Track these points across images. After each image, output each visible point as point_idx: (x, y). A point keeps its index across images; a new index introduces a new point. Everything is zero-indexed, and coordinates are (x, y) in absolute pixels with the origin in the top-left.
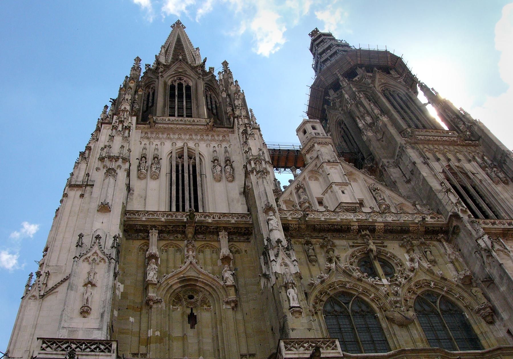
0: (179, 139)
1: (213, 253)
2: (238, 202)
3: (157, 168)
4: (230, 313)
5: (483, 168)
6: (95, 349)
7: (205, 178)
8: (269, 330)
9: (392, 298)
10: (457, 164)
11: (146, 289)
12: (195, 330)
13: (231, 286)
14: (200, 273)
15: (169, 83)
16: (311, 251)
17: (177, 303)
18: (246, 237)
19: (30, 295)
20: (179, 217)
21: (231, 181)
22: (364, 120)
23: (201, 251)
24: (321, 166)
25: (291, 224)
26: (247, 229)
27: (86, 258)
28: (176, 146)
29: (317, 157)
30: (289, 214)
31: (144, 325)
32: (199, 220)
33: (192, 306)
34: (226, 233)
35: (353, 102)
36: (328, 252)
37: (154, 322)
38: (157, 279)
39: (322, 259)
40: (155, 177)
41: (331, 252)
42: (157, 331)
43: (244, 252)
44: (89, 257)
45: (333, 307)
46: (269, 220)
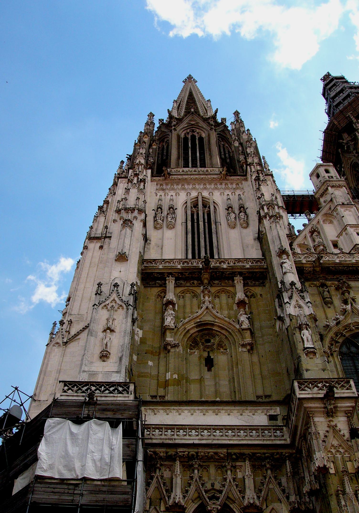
0: (194, 188)
1: (229, 297)
2: (252, 247)
3: (172, 217)
4: (246, 356)
6: (114, 390)
7: (219, 225)
8: (285, 371)
12: (212, 372)
15: (182, 136)
16: (326, 293)
17: (194, 347)
19: (54, 342)
20: (195, 264)
21: (246, 228)
23: (217, 296)
24: (335, 209)
25: (306, 267)
27: (105, 306)
28: (191, 196)
30: (303, 257)
32: (214, 266)
33: (209, 350)
34: (241, 278)
36: (343, 294)
37: (171, 366)
38: (174, 324)
39: (337, 301)
40: (171, 226)
41: (346, 294)
42: (175, 373)
43: (259, 296)
44: (108, 304)
45: (349, 349)
46: (283, 263)
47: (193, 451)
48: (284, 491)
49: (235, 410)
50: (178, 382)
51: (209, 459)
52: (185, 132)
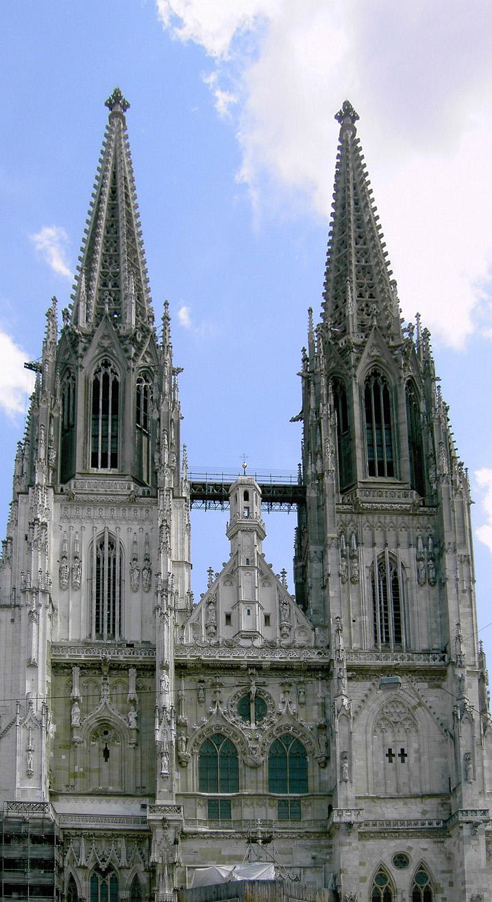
4: (132, 751)
5: (418, 560)
9: (251, 745)
10: (393, 550)
11: (72, 729)
13: (133, 729)
14: (111, 714)
15: (92, 379)
16: (201, 692)
18: (151, 673)
21: (147, 592)
22: (315, 464)
23: (114, 687)
26: (152, 666)
29: (237, 552)
31: (72, 761)
34: (135, 670)
35: (315, 419)
37: (78, 759)
39: (209, 700)
40: (76, 587)
41: (218, 694)
47: (91, 832)
48: (143, 858)
49: (122, 798)
50: (83, 775)
51: (101, 837)
52: (95, 368)
